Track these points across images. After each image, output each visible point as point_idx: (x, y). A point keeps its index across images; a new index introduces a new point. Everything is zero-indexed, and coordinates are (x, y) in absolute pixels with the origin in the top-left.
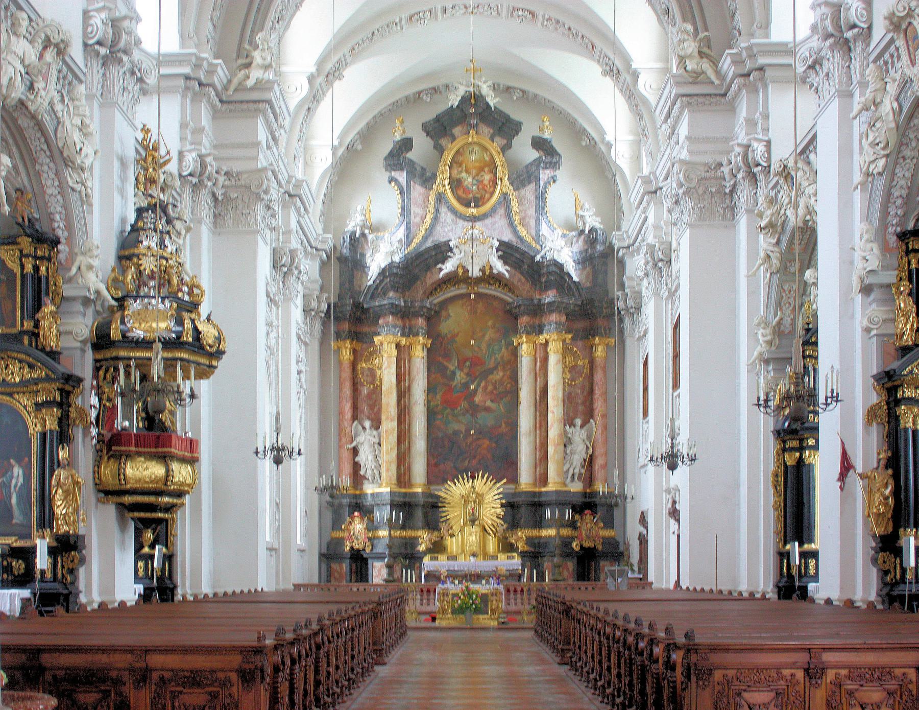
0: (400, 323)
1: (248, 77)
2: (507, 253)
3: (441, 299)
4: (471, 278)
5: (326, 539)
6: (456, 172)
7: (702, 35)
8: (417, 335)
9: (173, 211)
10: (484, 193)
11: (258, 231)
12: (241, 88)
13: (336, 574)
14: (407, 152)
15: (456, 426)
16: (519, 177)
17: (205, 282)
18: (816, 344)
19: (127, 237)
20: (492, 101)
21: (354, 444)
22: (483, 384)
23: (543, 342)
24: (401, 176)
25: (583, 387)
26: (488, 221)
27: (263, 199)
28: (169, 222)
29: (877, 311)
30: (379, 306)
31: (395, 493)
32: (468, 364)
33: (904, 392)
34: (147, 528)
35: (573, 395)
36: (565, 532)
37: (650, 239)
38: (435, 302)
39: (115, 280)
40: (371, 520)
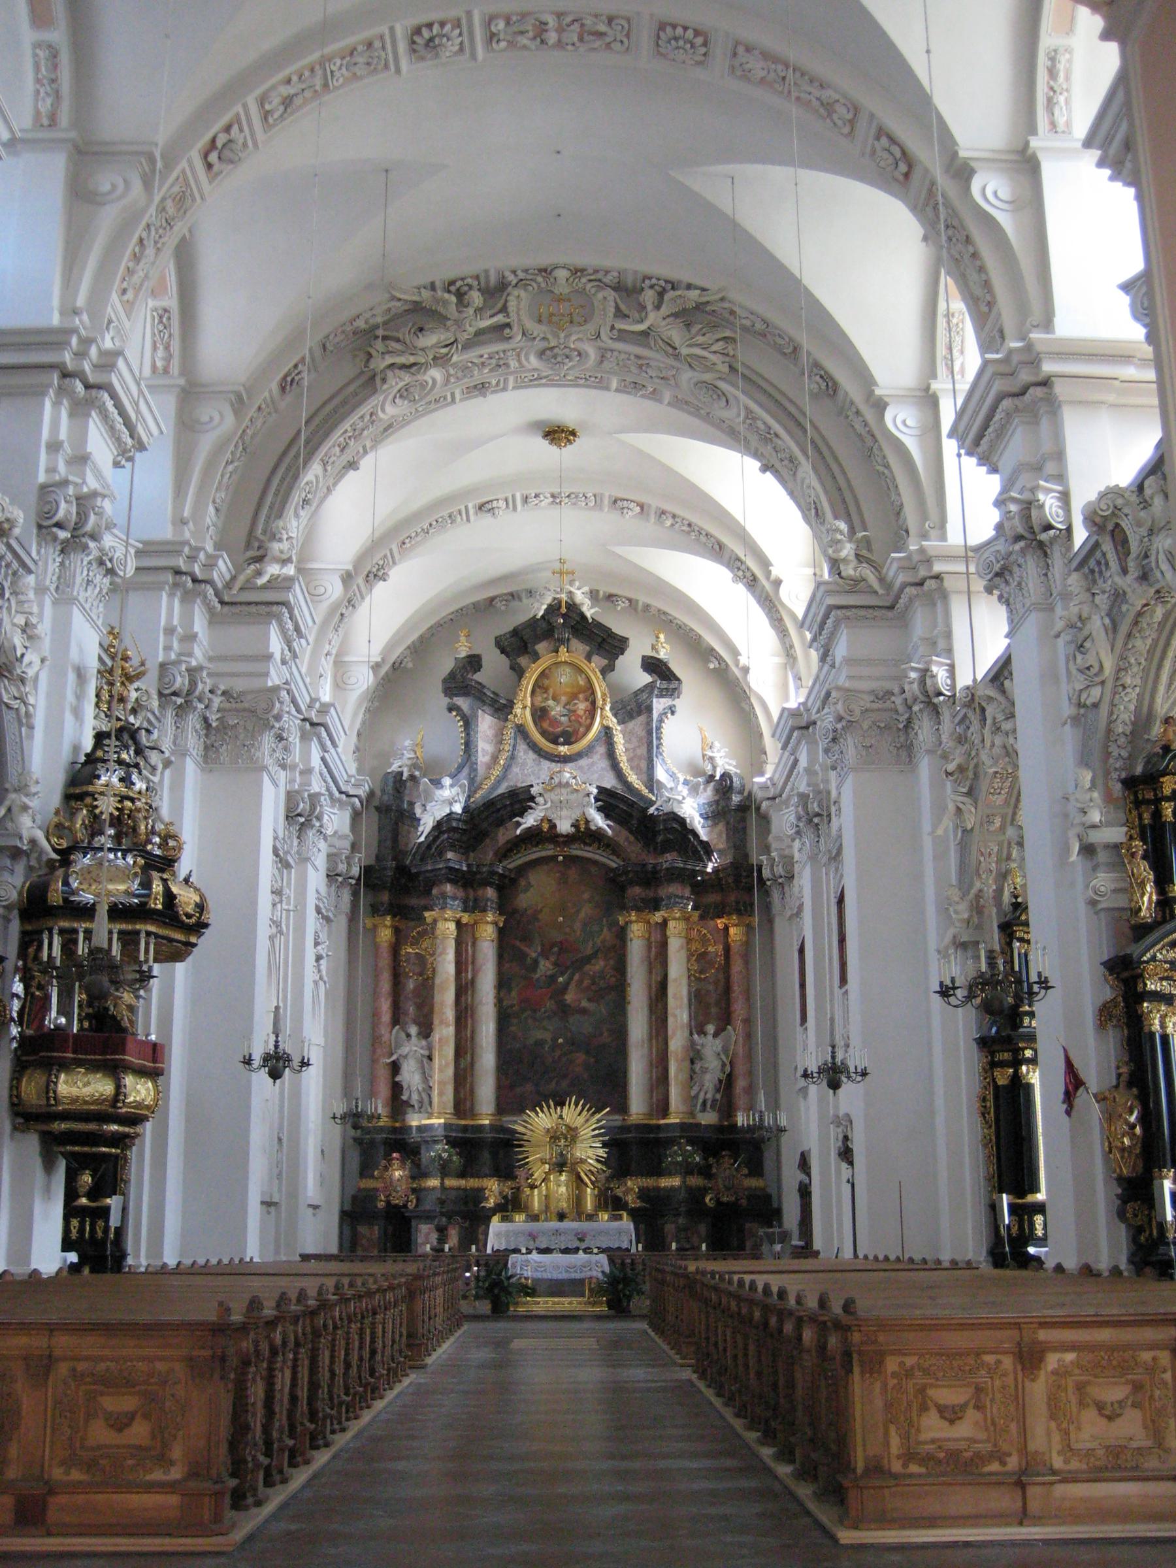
0: (460, 893)
1: (259, 573)
2: (611, 804)
3: (519, 862)
4: (563, 836)
5: (351, 1191)
6: (539, 699)
7: (860, 535)
8: (484, 910)
9: (148, 741)
10: (576, 725)
11: (264, 768)
12: (247, 587)
13: (364, 1241)
14: (475, 672)
15: (539, 1035)
16: (624, 707)
17: (189, 833)
18: (1026, 924)
19: (79, 771)
20: (589, 611)
21: (394, 1058)
22: (577, 977)
23: (659, 920)
24: (463, 702)
25: (716, 983)
26: (583, 762)
27: (273, 727)
28: (139, 752)
29: (1104, 881)
30: (433, 870)
31: (451, 1125)
32: (556, 949)
33: (1145, 985)
34: (85, 1169)
35: (703, 992)
36: (695, 1181)
37: (803, 787)
38: (510, 866)
39: (59, 826)
40: (417, 1165)
